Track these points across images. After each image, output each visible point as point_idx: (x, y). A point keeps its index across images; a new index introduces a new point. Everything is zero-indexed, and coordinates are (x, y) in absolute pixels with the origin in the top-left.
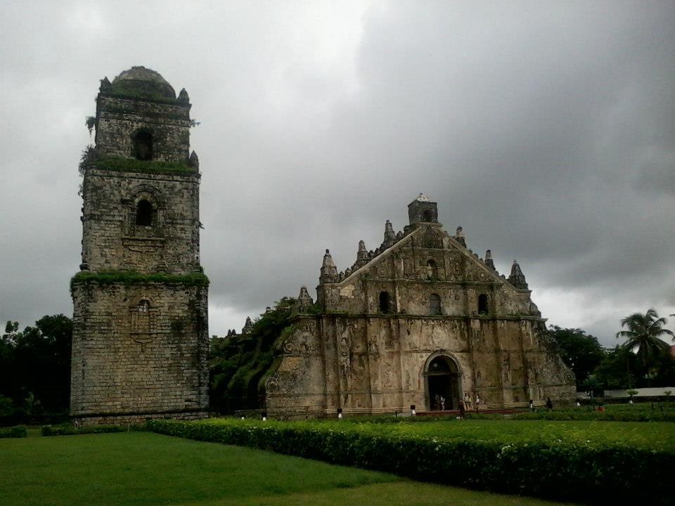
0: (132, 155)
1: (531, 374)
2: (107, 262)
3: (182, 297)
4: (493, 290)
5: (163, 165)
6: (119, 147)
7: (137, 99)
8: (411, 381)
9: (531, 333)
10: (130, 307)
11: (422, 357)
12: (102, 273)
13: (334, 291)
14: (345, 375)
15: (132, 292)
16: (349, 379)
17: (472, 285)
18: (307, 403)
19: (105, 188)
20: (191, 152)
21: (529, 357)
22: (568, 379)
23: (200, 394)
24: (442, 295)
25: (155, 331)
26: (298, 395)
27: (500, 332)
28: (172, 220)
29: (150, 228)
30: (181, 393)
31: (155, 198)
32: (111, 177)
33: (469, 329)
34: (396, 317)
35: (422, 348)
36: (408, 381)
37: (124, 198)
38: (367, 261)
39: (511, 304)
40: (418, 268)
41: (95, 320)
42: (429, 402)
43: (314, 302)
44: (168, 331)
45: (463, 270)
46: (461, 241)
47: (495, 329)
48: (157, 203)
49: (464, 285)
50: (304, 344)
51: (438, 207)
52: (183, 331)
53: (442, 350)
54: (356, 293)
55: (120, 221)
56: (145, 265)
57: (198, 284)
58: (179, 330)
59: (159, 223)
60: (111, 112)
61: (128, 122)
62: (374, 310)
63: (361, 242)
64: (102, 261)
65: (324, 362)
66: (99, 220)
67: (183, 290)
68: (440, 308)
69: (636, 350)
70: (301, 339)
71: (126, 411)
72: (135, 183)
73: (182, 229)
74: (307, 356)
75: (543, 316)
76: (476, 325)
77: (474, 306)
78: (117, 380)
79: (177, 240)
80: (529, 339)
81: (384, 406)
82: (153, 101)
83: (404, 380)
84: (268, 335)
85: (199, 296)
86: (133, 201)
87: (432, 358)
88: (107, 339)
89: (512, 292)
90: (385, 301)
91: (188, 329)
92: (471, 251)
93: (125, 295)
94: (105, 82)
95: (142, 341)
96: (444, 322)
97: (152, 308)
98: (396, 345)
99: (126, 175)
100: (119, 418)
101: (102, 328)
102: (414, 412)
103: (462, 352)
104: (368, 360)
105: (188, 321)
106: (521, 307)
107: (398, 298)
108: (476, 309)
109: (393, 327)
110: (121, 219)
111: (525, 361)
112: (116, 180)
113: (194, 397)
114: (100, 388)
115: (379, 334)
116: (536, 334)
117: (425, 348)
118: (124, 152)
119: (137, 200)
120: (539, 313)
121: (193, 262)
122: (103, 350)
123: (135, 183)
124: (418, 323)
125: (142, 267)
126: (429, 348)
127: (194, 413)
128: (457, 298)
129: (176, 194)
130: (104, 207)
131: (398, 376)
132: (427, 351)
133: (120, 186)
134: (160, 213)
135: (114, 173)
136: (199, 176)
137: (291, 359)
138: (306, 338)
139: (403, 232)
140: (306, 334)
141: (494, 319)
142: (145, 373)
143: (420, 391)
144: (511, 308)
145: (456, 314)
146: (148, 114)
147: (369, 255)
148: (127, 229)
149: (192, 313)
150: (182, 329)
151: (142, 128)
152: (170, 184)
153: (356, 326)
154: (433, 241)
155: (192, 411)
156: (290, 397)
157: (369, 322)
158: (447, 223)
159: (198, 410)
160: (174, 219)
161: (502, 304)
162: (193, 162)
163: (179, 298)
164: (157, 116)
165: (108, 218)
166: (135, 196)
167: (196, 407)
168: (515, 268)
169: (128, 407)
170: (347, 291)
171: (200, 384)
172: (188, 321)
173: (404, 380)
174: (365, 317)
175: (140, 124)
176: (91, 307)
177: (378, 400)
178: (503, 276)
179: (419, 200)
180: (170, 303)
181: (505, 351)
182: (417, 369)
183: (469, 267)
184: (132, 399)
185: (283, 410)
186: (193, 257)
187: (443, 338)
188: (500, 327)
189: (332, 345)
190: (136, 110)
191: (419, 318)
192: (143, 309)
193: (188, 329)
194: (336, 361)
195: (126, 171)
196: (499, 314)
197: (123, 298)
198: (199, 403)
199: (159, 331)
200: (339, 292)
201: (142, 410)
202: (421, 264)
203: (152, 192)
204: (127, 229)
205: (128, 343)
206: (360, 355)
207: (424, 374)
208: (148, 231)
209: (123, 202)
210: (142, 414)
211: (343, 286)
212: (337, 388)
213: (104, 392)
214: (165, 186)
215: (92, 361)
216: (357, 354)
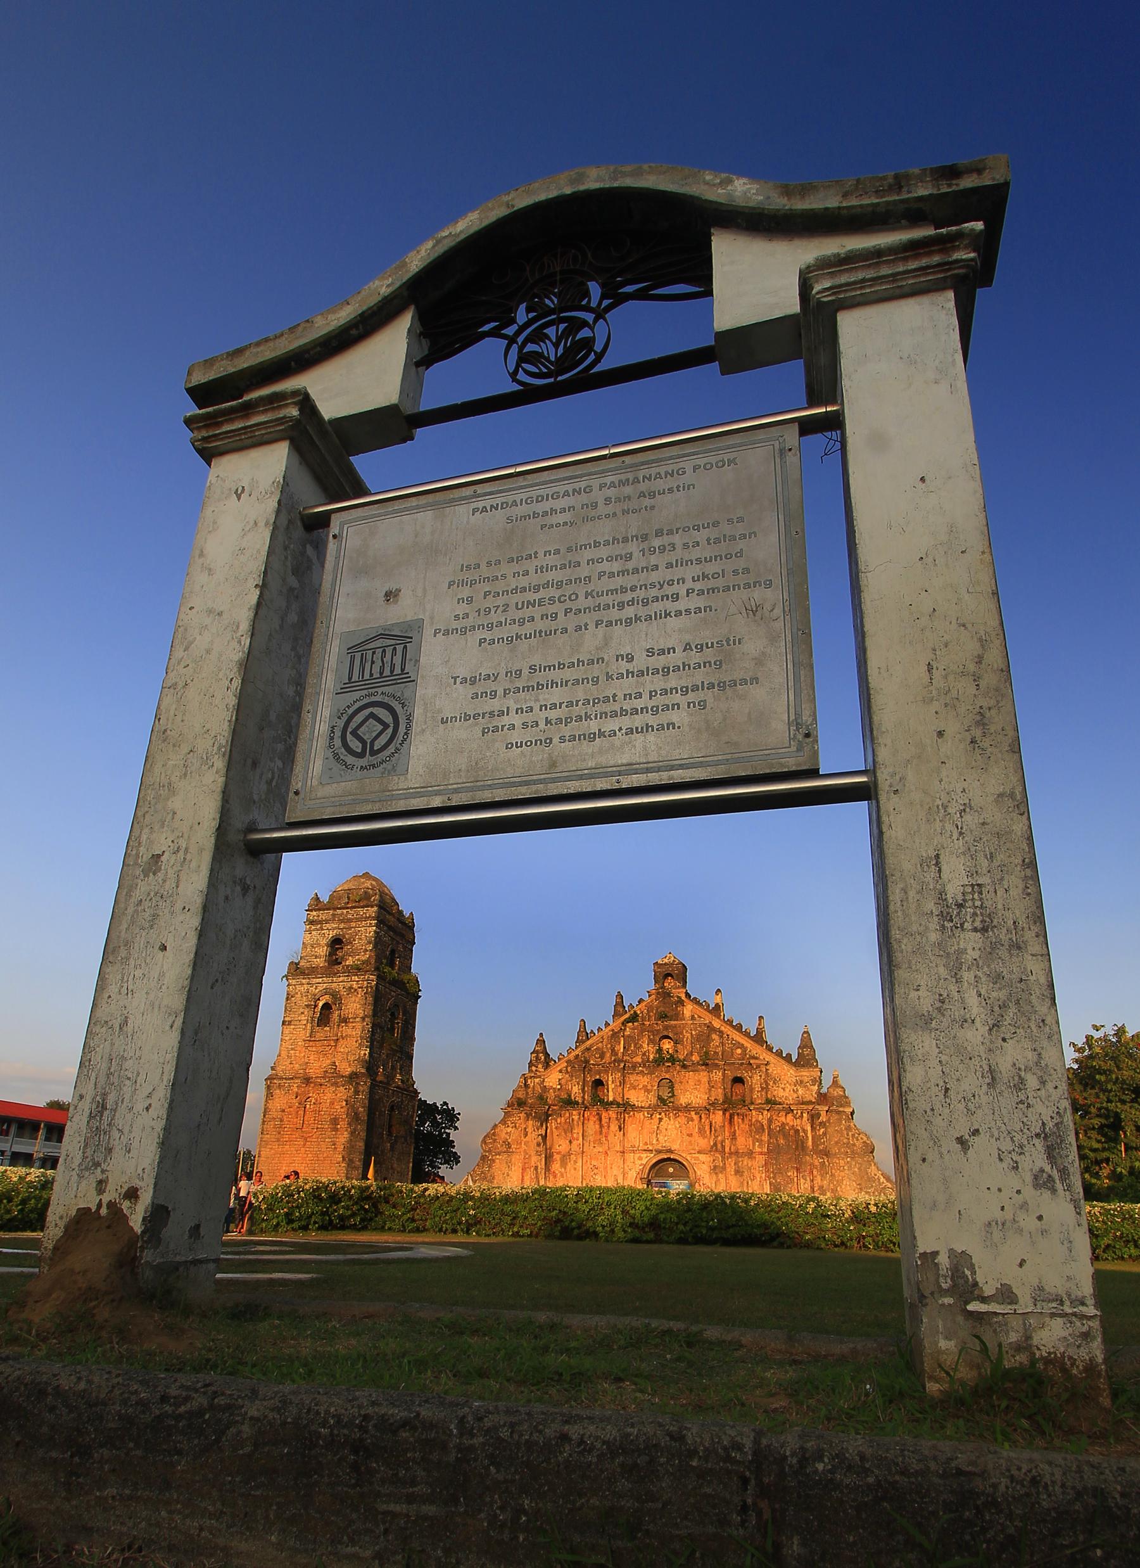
9: (809, 1128)
11: (640, 1158)
53: (670, 1151)
56: (317, 1066)
66: (290, 1023)
77: (718, 1094)
87: (654, 1161)
89: (789, 1073)
103: (699, 1152)
107: (611, 1086)
109: (604, 1121)
119: (321, 1004)
140: (509, 1130)
146: (342, 921)
164: (350, 921)
170: (553, 1079)
179: (660, 962)
187: (672, 1134)
193: (343, 1124)
202: (651, 1041)
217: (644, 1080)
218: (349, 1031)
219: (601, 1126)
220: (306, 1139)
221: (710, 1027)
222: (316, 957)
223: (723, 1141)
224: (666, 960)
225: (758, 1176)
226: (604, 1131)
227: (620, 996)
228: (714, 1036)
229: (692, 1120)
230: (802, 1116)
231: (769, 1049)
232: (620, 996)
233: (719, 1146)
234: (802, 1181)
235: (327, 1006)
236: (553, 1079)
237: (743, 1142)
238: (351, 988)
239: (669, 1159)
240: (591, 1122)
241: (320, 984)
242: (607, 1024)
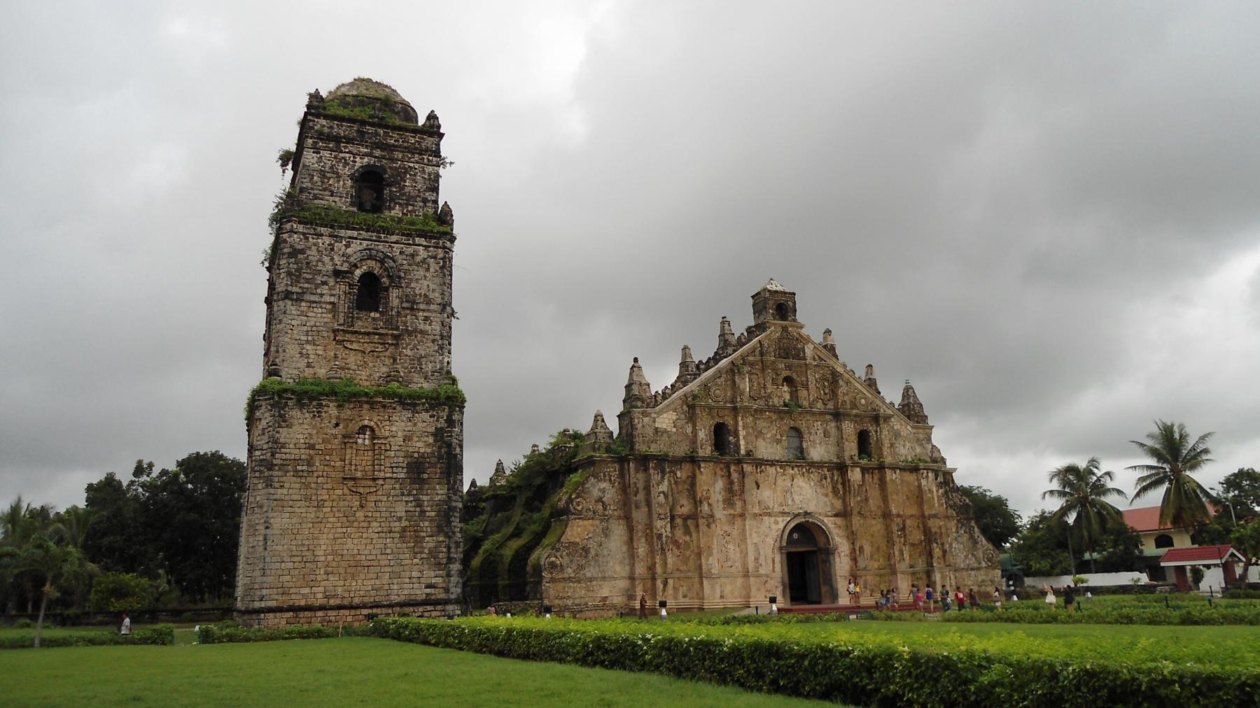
0: (352, 204)
1: (937, 552)
2: (309, 365)
3: (425, 422)
4: (878, 425)
5: (400, 220)
6: (332, 192)
7: (363, 123)
10: (344, 437)
11: (776, 523)
12: (302, 382)
14: (663, 549)
15: (346, 413)
16: (669, 555)
17: (849, 415)
18: (605, 592)
19: (308, 252)
20: (441, 203)
21: (934, 524)
22: (989, 560)
23: (449, 575)
24: (804, 429)
25: (382, 474)
26: (591, 580)
27: (890, 487)
28: (412, 305)
30: (419, 575)
31: (386, 270)
33: (845, 482)
34: (739, 462)
36: (757, 559)
37: (339, 268)
38: (696, 376)
40: (770, 388)
41: (288, 456)
42: (788, 591)
43: (615, 436)
44: (403, 475)
45: (834, 393)
46: (831, 349)
47: (883, 483)
48: (389, 277)
49: (837, 416)
50: (600, 500)
52: (425, 476)
53: (806, 513)
54: (679, 423)
55: (332, 303)
57: (449, 402)
58: (419, 473)
59: (392, 308)
62: (706, 450)
65: (631, 530)
67: (427, 411)
68: (801, 450)
69: (1071, 518)
70: (596, 493)
71: (332, 602)
72: (356, 247)
73: (426, 318)
74: (605, 518)
75: (949, 465)
76: (855, 475)
77: (851, 448)
78: (319, 552)
81: (722, 597)
82: (387, 127)
83: (751, 558)
84: (546, 481)
85: (450, 422)
86: (352, 273)
87: (792, 525)
88: (307, 486)
89: (905, 428)
92: (845, 366)
93: (338, 418)
94: (315, 97)
95: (361, 490)
96: (808, 471)
97: (379, 438)
98: (739, 504)
99: (342, 233)
100: (320, 614)
101: (299, 468)
102: (774, 607)
103: (836, 515)
104: (697, 526)
105: (434, 460)
106: (918, 450)
107: (742, 433)
108: (855, 452)
109: (735, 476)
111: (927, 532)
112: (327, 240)
113: (439, 580)
114: (290, 565)
115: (712, 484)
118: (340, 198)
119: (358, 273)
120: (943, 461)
121: (441, 369)
122: (298, 504)
123: (356, 247)
124: (771, 470)
125: (364, 374)
127: (439, 607)
128: (826, 434)
129: (418, 265)
130: (307, 281)
131: (741, 552)
132: (783, 513)
133: (332, 249)
134: (394, 294)
136: (452, 239)
137: (581, 522)
138: (603, 491)
141: (881, 468)
142: (364, 541)
143: (774, 575)
144: (906, 451)
145: (826, 459)
147: (698, 367)
149: (440, 448)
151: (368, 165)
152: (410, 250)
153: (679, 474)
154: (791, 348)
155: (436, 603)
156: (579, 582)
157: (699, 467)
159: (447, 602)
160: (414, 302)
161: (892, 445)
162: (445, 218)
163: (420, 424)
164: (390, 148)
165: (313, 298)
166: (356, 266)
167: (443, 596)
168: (908, 392)
171: (450, 560)
172: (434, 460)
173: (751, 558)
174: (693, 460)
175: (366, 160)
176: (283, 434)
177: (712, 588)
178: (892, 404)
180: (406, 432)
181: (899, 516)
183: (843, 389)
184: (341, 583)
185: (569, 602)
186: (442, 362)
187: (809, 496)
189: (643, 504)
191: (772, 463)
192: (364, 440)
194: (650, 526)
195: (341, 228)
196: (888, 460)
197: (334, 421)
198: (447, 590)
201: (356, 601)
202: (774, 382)
205: (339, 492)
206: (685, 518)
207: (781, 548)
208: (374, 319)
209: (337, 273)
210: (357, 607)
211: (660, 413)
212: (651, 568)
213: (297, 572)
214: (401, 253)
215: (280, 521)
216: (680, 516)
226: (736, 487)
228: (841, 382)
235: (369, 278)
238: (413, 256)
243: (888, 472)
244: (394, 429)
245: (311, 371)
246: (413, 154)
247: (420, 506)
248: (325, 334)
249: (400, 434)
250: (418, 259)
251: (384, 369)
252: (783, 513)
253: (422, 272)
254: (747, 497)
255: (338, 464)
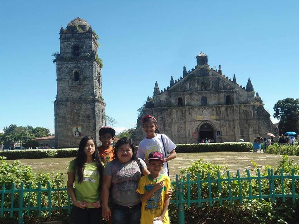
2: (64, 95)
3: (89, 106)
8: (191, 134)
9: (252, 111)
11: (197, 124)
13: (157, 98)
29: (78, 82)
32: (64, 64)
33: (220, 112)
35: (197, 120)
36: (189, 134)
39: (243, 99)
51: (208, 57)
52: (90, 118)
53: (206, 121)
58: (89, 118)
60: (64, 40)
61: (70, 43)
63: (171, 77)
64: (62, 95)
66: (61, 80)
67: (89, 103)
71: (72, 146)
72: (72, 65)
73: (89, 81)
77: (223, 101)
79: (88, 85)
80: (252, 114)
87: (202, 124)
88: (65, 122)
89: (246, 93)
90: (180, 102)
91: (91, 118)
92: (224, 76)
93: (70, 107)
103: (216, 121)
107: (186, 99)
109: (183, 111)
110: (68, 79)
114: (63, 139)
116: (256, 112)
117: (199, 120)
119: (73, 72)
124: (196, 109)
126: (200, 120)
129: (87, 68)
135: (65, 63)
139: (191, 71)
148: (70, 83)
150: (90, 117)
158: (212, 64)
164: (80, 39)
168: (249, 82)
169: (73, 145)
175: (74, 43)
179: (199, 55)
182: (194, 129)
188: (236, 110)
190: (73, 37)
191: (196, 107)
197: (69, 108)
199: (82, 119)
200: (160, 98)
202: (198, 83)
203: (79, 67)
204: (70, 83)
207: (198, 130)
214: (83, 66)
217: (196, 97)
218: (88, 82)
219: (183, 114)
220: (76, 124)
221: (219, 79)
222: (67, 53)
223: (225, 117)
224: (201, 55)
225: (236, 127)
226: (184, 115)
227: (184, 68)
228: (220, 82)
229: (214, 110)
230: (250, 108)
231: (238, 85)
232: (184, 68)
233: (224, 118)
234: (250, 128)
236: (163, 98)
237: (230, 117)
239: (206, 123)
240: (179, 113)
241: (72, 64)
242: (181, 78)
243: (235, 107)
244: (83, 108)
245: (65, 96)
246: (85, 39)
247: (89, 125)
248: (67, 88)
249: (84, 109)
250: (87, 66)
251: (80, 94)
252: (198, 121)
253: (88, 70)
254: (186, 117)
255: (71, 117)
